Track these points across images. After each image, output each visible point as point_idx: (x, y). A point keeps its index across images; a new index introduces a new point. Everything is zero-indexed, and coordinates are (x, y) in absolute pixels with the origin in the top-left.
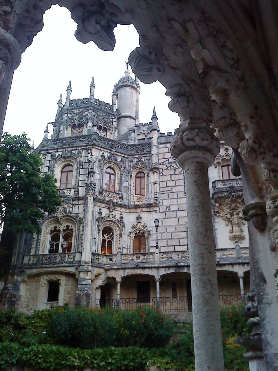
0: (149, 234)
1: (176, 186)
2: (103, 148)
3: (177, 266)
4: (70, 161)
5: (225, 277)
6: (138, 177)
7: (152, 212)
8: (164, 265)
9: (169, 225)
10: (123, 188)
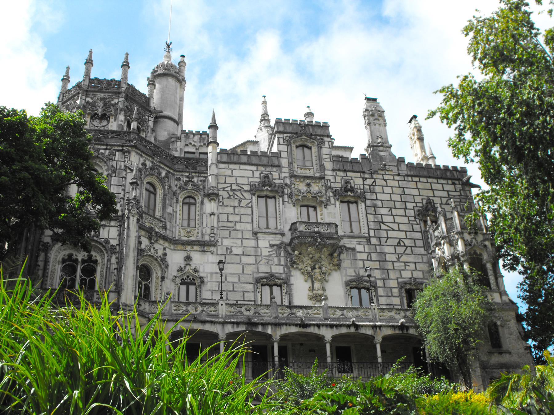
0: (203, 282)
1: (241, 222)
2: (144, 153)
3: (250, 324)
5: (302, 344)
6: (186, 203)
7: (206, 253)
8: (232, 320)
9: (230, 272)
10: (166, 214)
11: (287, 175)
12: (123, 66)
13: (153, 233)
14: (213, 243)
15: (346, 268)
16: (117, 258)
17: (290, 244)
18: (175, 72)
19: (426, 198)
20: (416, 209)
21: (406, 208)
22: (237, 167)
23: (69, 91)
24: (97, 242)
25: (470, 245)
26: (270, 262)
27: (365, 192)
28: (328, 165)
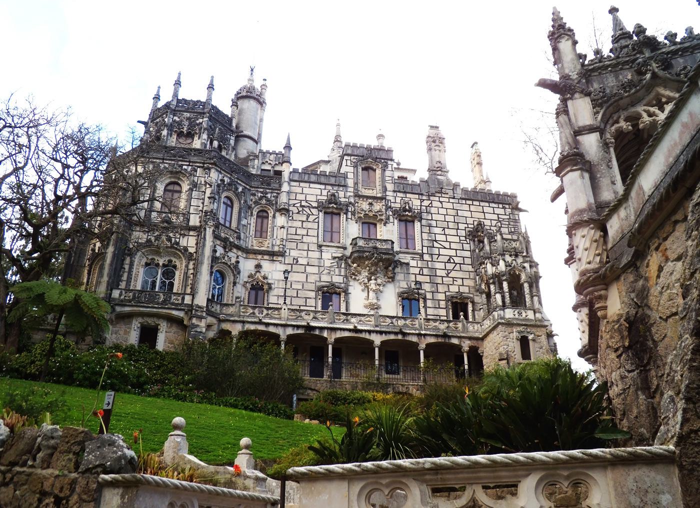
0: (270, 288)
1: (307, 235)
2: (223, 170)
3: (309, 328)
4: (179, 179)
11: (352, 194)
12: (209, 87)
13: (228, 242)
14: (282, 254)
15: (399, 281)
16: (194, 264)
17: (350, 257)
18: (257, 95)
19: (477, 220)
20: (467, 229)
21: (458, 229)
22: (307, 185)
23: (159, 109)
24: (176, 249)
25: (511, 266)
26: (332, 273)
27: (421, 213)
28: (390, 187)
